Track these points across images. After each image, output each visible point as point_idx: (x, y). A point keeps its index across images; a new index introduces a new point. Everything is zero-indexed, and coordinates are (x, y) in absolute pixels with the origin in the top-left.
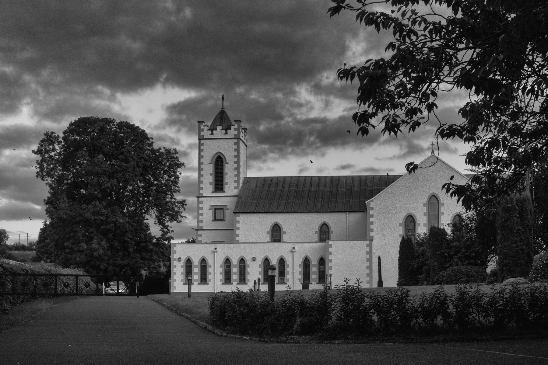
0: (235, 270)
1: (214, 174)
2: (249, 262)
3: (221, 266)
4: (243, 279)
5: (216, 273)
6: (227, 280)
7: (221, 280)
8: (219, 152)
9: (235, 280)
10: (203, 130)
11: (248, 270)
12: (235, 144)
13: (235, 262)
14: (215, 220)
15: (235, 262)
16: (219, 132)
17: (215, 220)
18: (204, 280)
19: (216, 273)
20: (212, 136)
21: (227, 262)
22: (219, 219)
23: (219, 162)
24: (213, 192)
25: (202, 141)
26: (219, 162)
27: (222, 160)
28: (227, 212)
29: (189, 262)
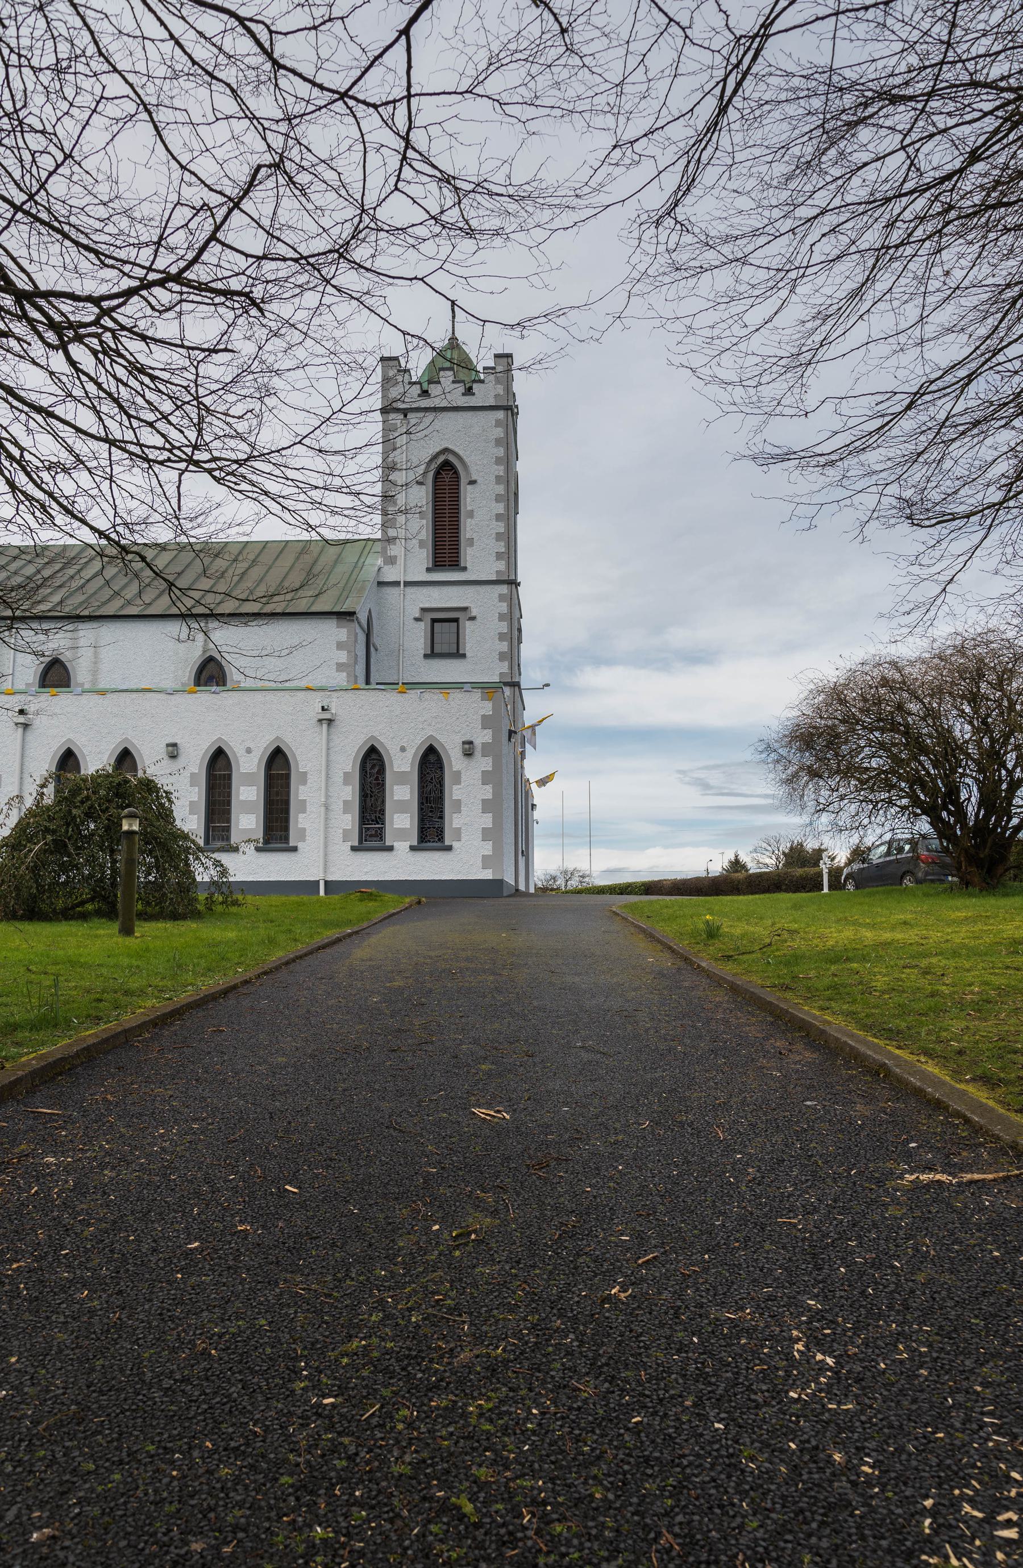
0: (402, 794)
1: (430, 516)
2: (454, 760)
4: (431, 832)
5: (323, 807)
6: (371, 830)
8: (446, 450)
9: (402, 834)
11: (453, 792)
12: (498, 424)
14: (432, 654)
17: (432, 654)
19: (323, 807)
20: (425, 403)
21: (372, 764)
22: (445, 650)
24: (428, 570)
26: (446, 477)
27: (456, 472)
28: (469, 628)
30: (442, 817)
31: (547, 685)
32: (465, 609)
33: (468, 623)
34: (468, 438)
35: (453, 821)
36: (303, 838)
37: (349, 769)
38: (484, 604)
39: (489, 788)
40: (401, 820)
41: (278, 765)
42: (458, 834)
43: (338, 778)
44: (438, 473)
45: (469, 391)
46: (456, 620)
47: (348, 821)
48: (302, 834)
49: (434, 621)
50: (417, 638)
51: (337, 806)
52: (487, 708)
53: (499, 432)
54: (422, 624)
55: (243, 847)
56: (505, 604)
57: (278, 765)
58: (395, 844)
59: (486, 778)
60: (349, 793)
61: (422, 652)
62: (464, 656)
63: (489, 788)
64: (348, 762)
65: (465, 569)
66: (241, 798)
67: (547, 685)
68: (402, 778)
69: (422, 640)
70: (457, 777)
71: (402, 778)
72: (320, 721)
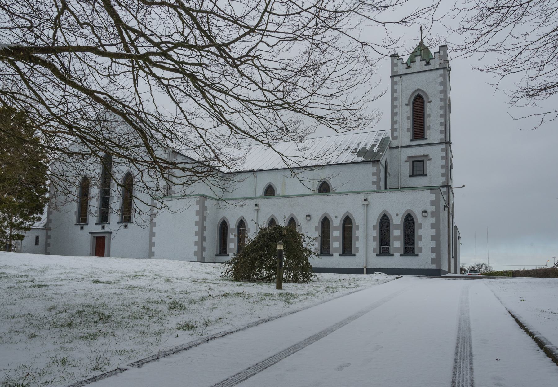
0: (397, 233)
1: (411, 118)
2: (419, 219)
3: (375, 227)
6: (384, 248)
7: (374, 250)
8: (418, 90)
9: (397, 250)
10: (396, 65)
11: (419, 232)
13: (397, 220)
14: (413, 175)
15: (397, 220)
16: (418, 65)
18: (348, 248)
21: (385, 222)
23: (418, 102)
24: (411, 141)
25: (396, 79)
28: (428, 163)
29: (325, 223)
30: (414, 243)
31: (464, 186)
32: (427, 156)
33: (428, 162)
34: (427, 83)
35: (419, 244)
36: (357, 251)
37: (375, 223)
38: (436, 154)
39: (434, 230)
40: (397, 244)
41: (348, 222)
42: (420, 250)
43: (371, 227)
44: (415, 100)
45: (428, 64)
46: (423, 161)
47: (374, 245)
48: (357, 249)
49: (413, 162)
50: (406, 169)
51: (371, 239)
52: (433, 197)
53: (441, 79)
54: (408, 163)
55: (334, 254)
56: (444, 153)
57: (348, 222)
58: (394, 254)
59: (433, 226)
60: (375, 233)
61: (409, 175)
62: (426, 175)
63: (434, 230)
64: (374, 220)
65: (427, 139)
66: (334, 236)
67: (464, 186)
68: (397, 227)
69: (408, 170)
70: (420, 226)
71: (397, 227)
72: (364, 205)
